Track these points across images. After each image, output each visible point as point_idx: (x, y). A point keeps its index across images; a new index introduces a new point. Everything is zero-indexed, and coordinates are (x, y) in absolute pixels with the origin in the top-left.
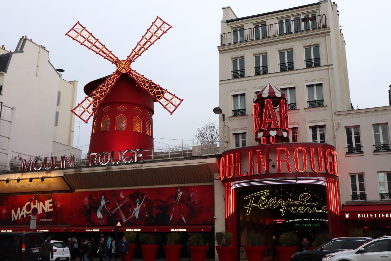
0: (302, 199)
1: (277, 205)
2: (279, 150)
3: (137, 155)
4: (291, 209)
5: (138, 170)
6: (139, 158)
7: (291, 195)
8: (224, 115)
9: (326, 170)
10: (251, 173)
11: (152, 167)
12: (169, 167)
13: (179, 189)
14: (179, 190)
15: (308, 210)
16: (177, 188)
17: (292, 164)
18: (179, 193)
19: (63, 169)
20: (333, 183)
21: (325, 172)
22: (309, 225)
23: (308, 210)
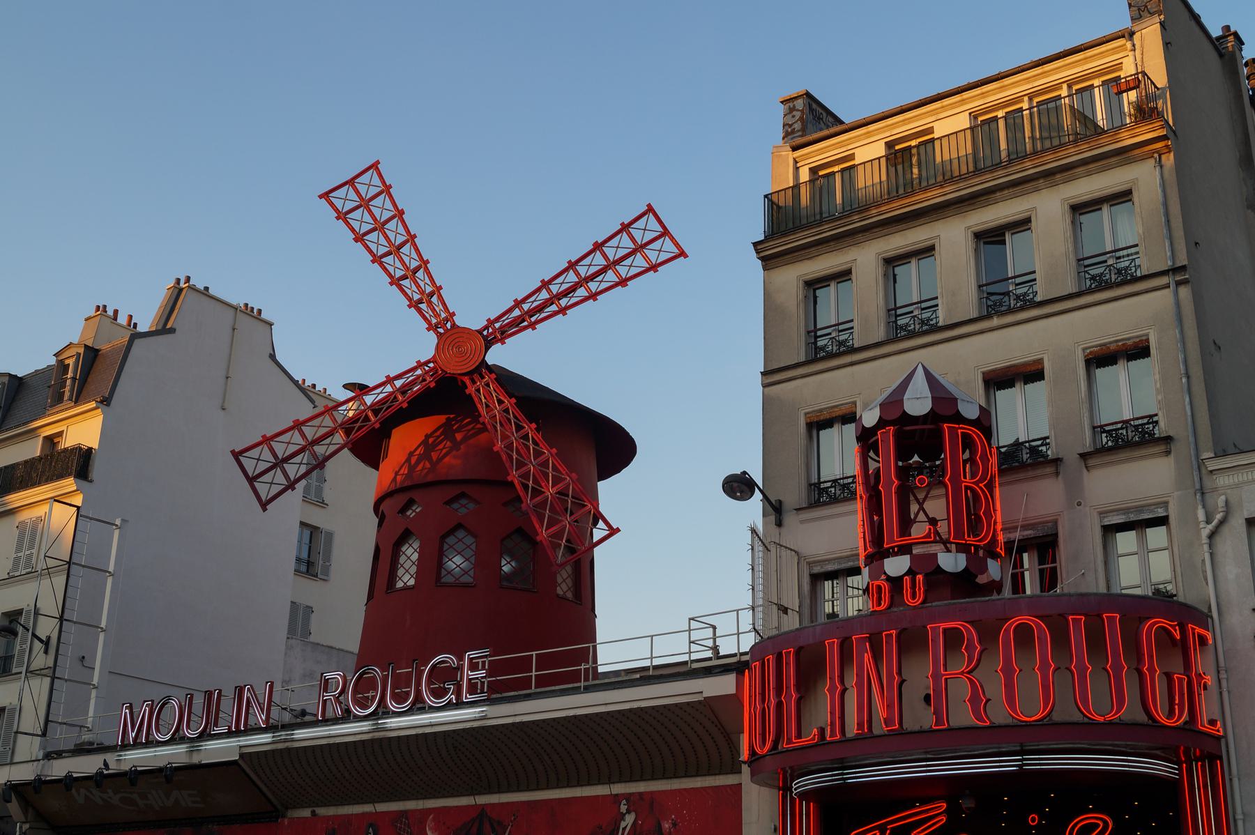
3: (468, 674)
5: (473, 729)
8: (775, 510)
9: (1145, 711)
10: (833, 734)
11: (518, 719)
12: (575, 717)
13: (624, 802)
14: (623, 808)
16: (617, 798)
17: (995, 688)
18: (622, 817)
21: (1142, 718)
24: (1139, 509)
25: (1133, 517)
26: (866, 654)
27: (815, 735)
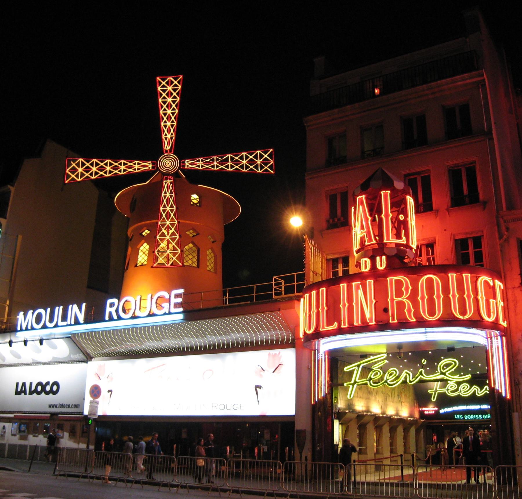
0: (444, 369)
2: (391, 281)
4: (448, 390)
6: (176, 305)
7: (424, 362)
15: (475, 391)
19: (71, 325)
20: (497, 339)
22: (478, 416)
23: (475, 391)
24: (471, 233)
25: (468, 236)
26: (359, 291)
27: (335, 325)
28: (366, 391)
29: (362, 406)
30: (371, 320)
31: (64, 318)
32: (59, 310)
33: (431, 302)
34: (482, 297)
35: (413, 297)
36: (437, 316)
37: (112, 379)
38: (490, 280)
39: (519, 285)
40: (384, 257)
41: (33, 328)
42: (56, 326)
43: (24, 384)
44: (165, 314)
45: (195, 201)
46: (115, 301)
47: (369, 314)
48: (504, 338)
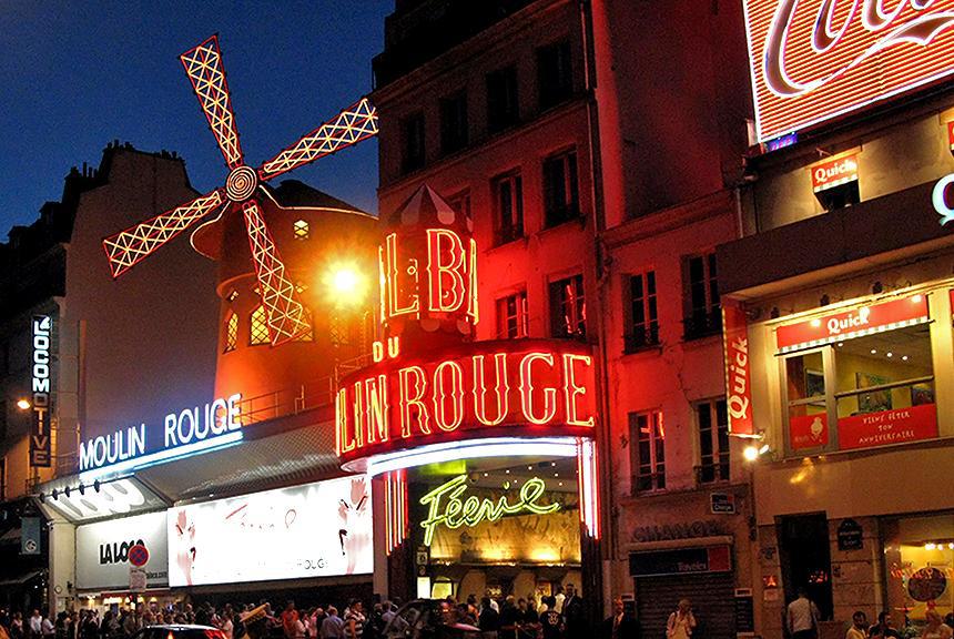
1: (482, 511)
2: (403, 373)
24: (568, 271)
25: (566, 276)
28: (514, 527)
29: (503, 552)
30: (383, 434)
31: (125, 451)
32: (119, 436)
33: (448, 401)
34: (526, 389)
35: (427, 399)
36: (457, 422)
37: (193, 533)
38: (549, 358)
39: (621, 355)
40: (396, 339)
41: (96, 467)
42: (118, 461)
43: (108, 546)
44: (224, 433)
45: (301, 232)
46: (172, 417)
47: (383, 427)
48: (594, 443)
